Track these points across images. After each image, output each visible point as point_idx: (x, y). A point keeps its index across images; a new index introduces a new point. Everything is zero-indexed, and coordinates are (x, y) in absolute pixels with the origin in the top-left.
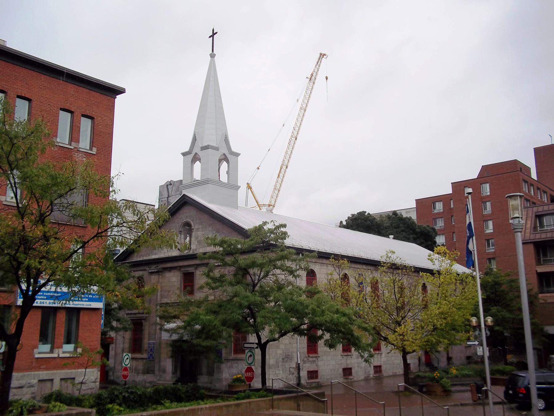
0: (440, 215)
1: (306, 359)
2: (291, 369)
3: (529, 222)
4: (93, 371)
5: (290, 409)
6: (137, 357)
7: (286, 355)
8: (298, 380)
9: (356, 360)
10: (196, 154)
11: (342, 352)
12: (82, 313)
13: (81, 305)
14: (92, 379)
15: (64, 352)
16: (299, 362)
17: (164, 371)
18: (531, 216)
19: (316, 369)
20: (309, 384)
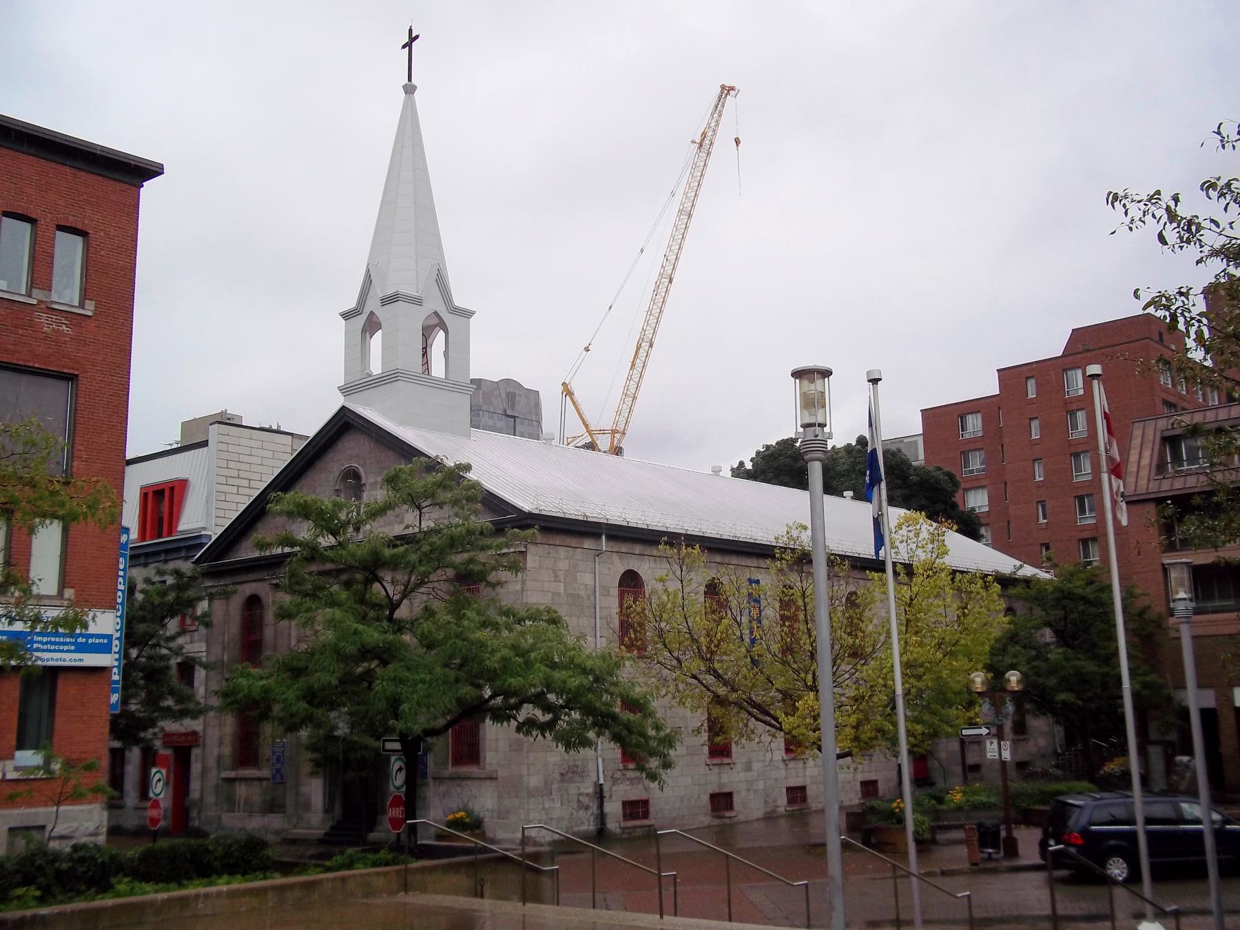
0: (974, 445)
1: (618, 775)
2: (581, 798)
3: (1147, 454)
4: (90, 812)
5: (456, 892)
6: (249, 776)
7: (569, 767)
8: (599, 823)
9: (742, 775)
10: (372, 313)
11: (707, 755)
12: (61, 682)
13: (57, 660)
14: (87, 828)
15: (17, 769)
16: (602, 781)
17: (307, 806)
18: (1151, 438)
19: (644, 797)
20: (627, 831)
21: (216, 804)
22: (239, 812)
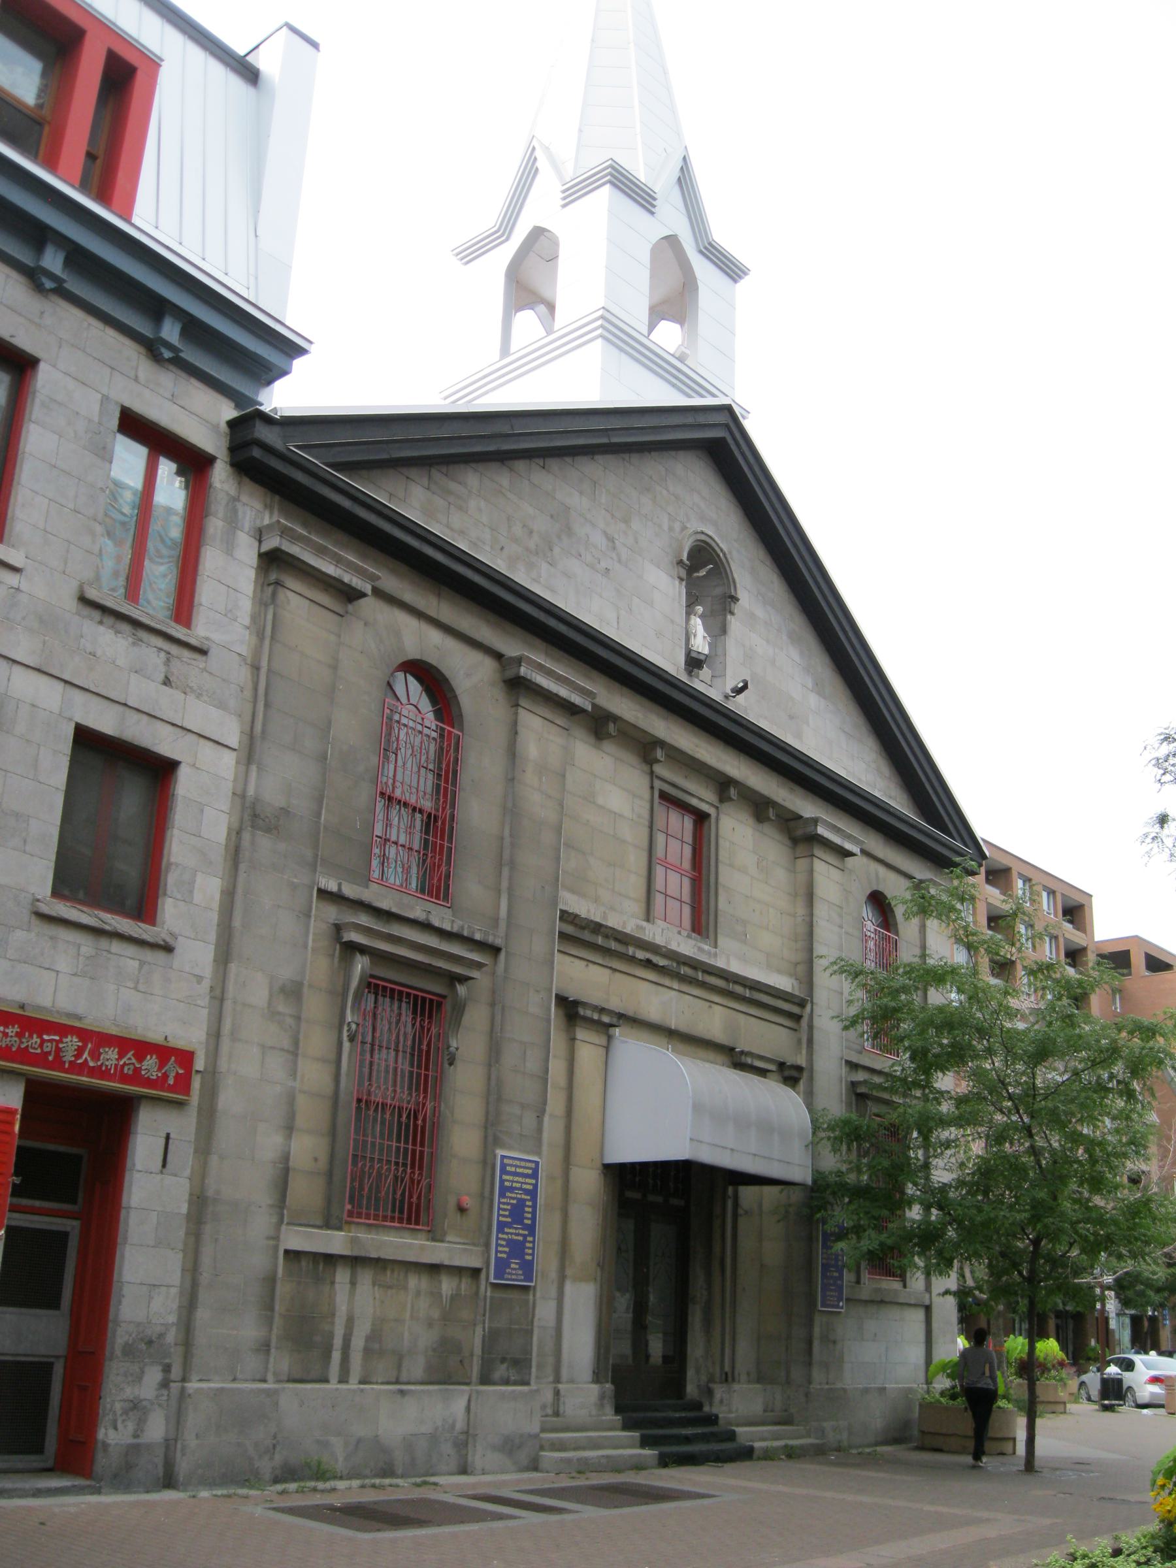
21: (264, 1348)
22: (343, 1380)
